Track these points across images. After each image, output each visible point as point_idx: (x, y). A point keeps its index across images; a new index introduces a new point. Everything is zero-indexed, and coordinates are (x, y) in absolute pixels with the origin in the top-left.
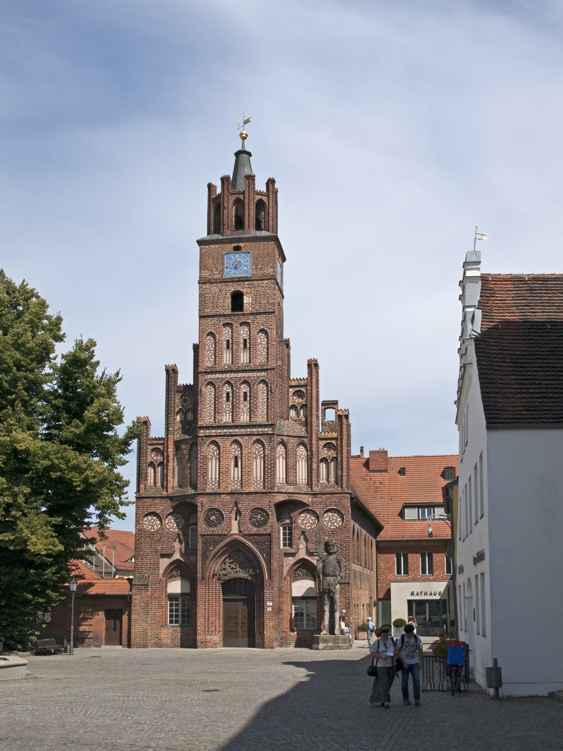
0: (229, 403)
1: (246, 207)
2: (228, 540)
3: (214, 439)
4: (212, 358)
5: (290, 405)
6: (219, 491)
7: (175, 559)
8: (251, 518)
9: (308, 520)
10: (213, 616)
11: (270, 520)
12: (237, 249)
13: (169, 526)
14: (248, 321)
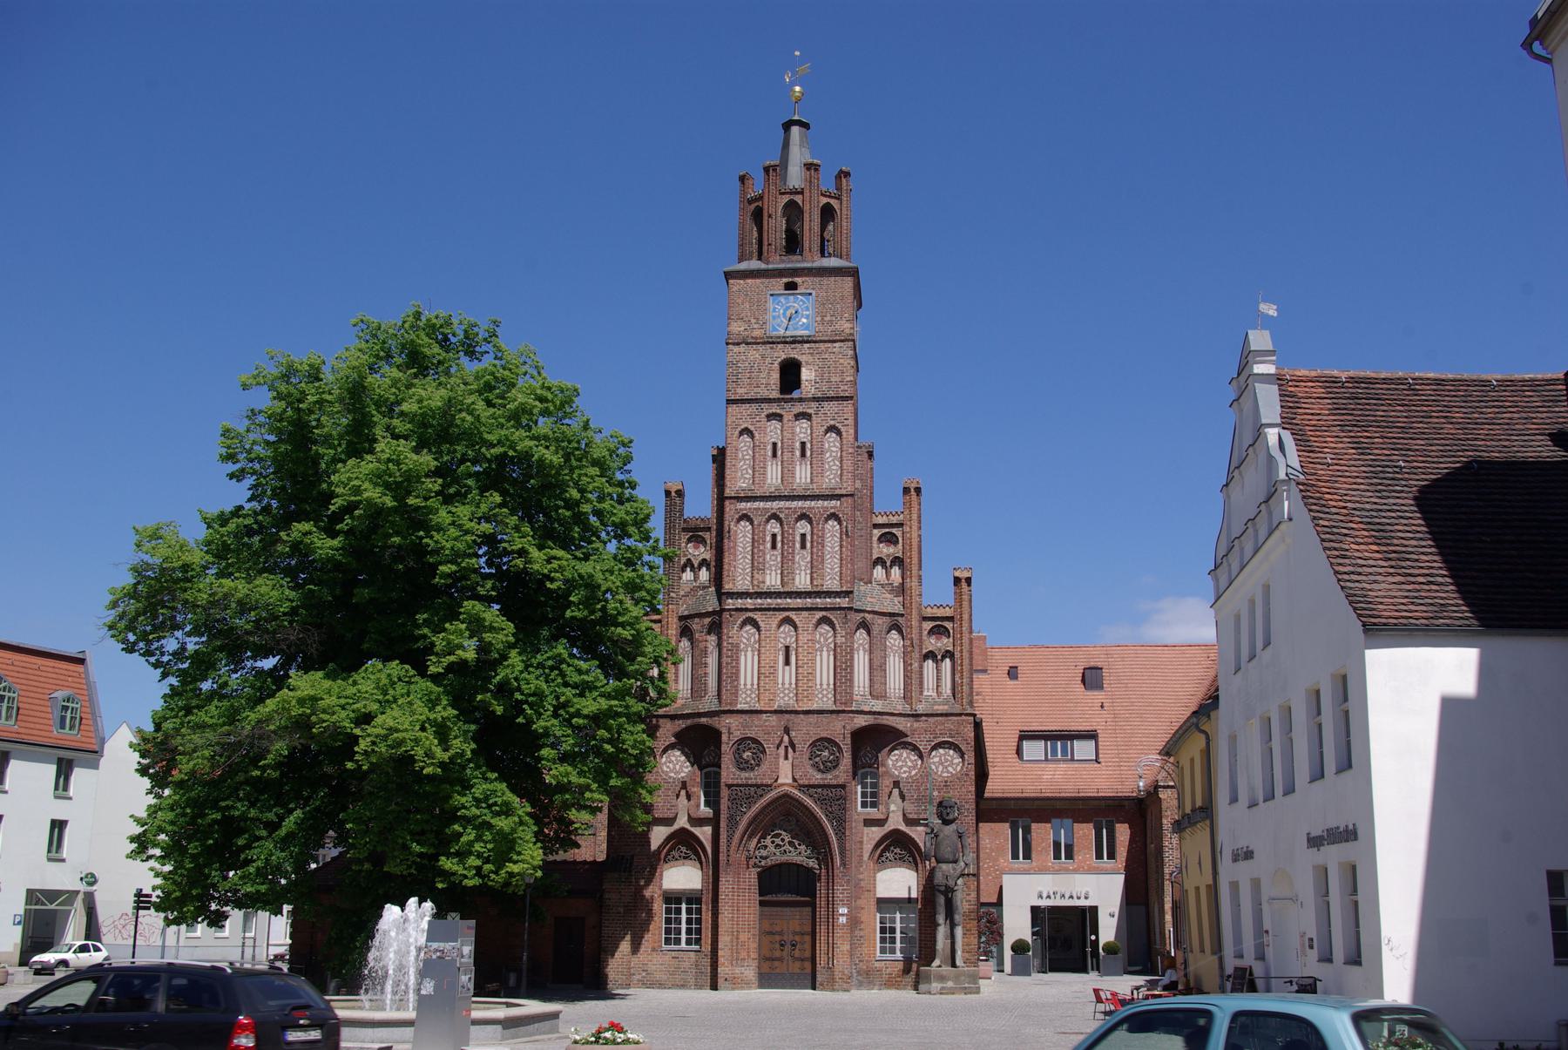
0: (775, 553)
1: (806, 216)
2: (773, 794)
3: (750, 614)
4: (747, 473)
5: (874, 557)
6: (758, 707)
9: (905, 761)
12: (791, 286)
13: (668, 767)
14: (809, 411)
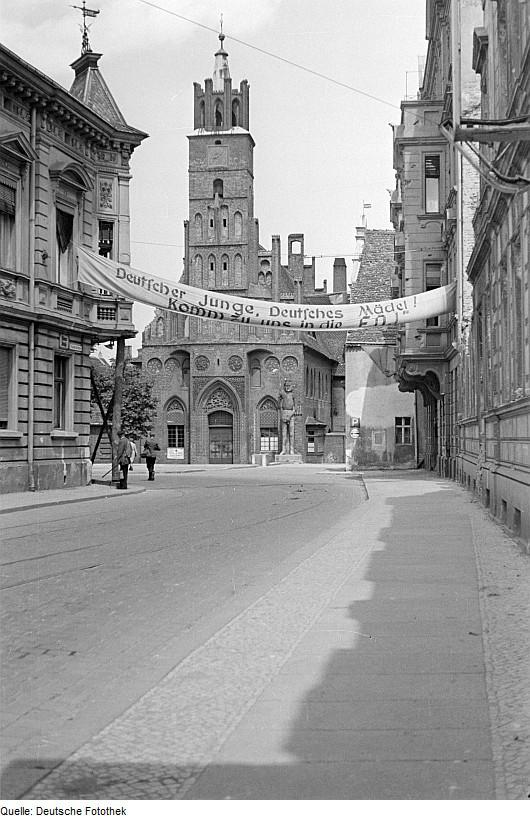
12: (218, 143)
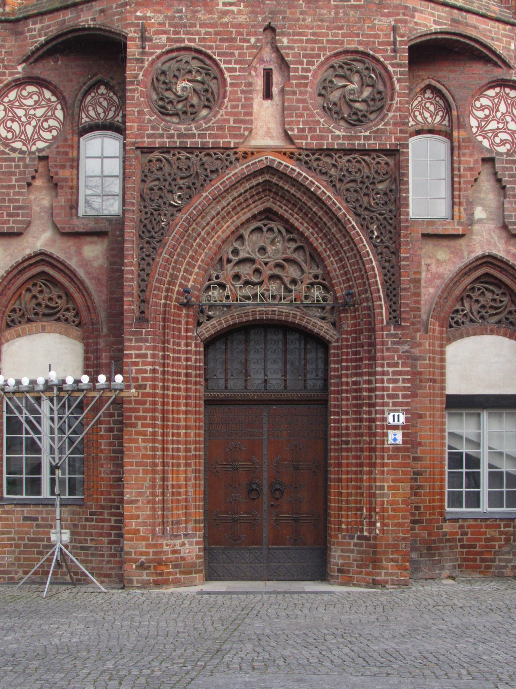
7: (28, 252)
8: (324, 88)
10: (179, 465)
11: (397, 99)
